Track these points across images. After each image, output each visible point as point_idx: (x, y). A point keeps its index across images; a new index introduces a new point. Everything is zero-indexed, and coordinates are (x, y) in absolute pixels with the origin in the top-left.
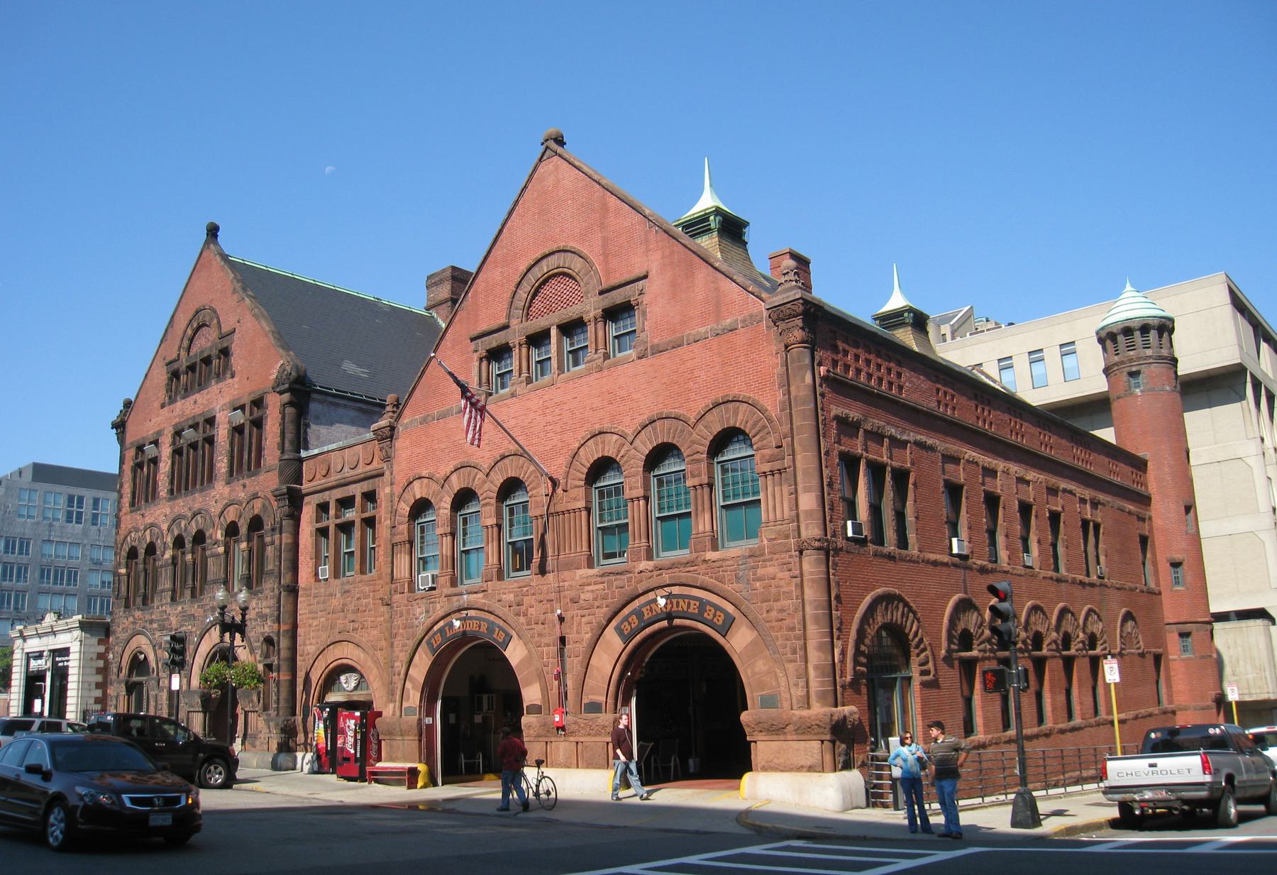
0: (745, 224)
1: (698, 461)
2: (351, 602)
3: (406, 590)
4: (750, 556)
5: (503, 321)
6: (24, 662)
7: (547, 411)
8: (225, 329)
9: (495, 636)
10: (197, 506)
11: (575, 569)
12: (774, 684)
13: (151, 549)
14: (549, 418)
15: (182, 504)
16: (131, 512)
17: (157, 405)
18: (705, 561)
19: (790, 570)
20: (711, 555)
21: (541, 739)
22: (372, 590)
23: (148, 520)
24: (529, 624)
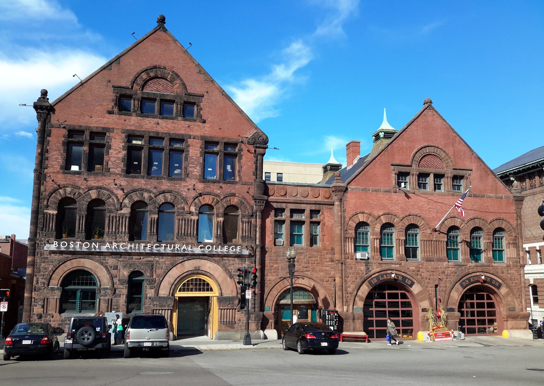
1: (490, 235)
2: (304, 258)
4: (507, 267)
5: (409, 163)
7: (430, 203)
9: (406, 282)
14: (431, 206)
18: (492, 266)
24: (422, 278)
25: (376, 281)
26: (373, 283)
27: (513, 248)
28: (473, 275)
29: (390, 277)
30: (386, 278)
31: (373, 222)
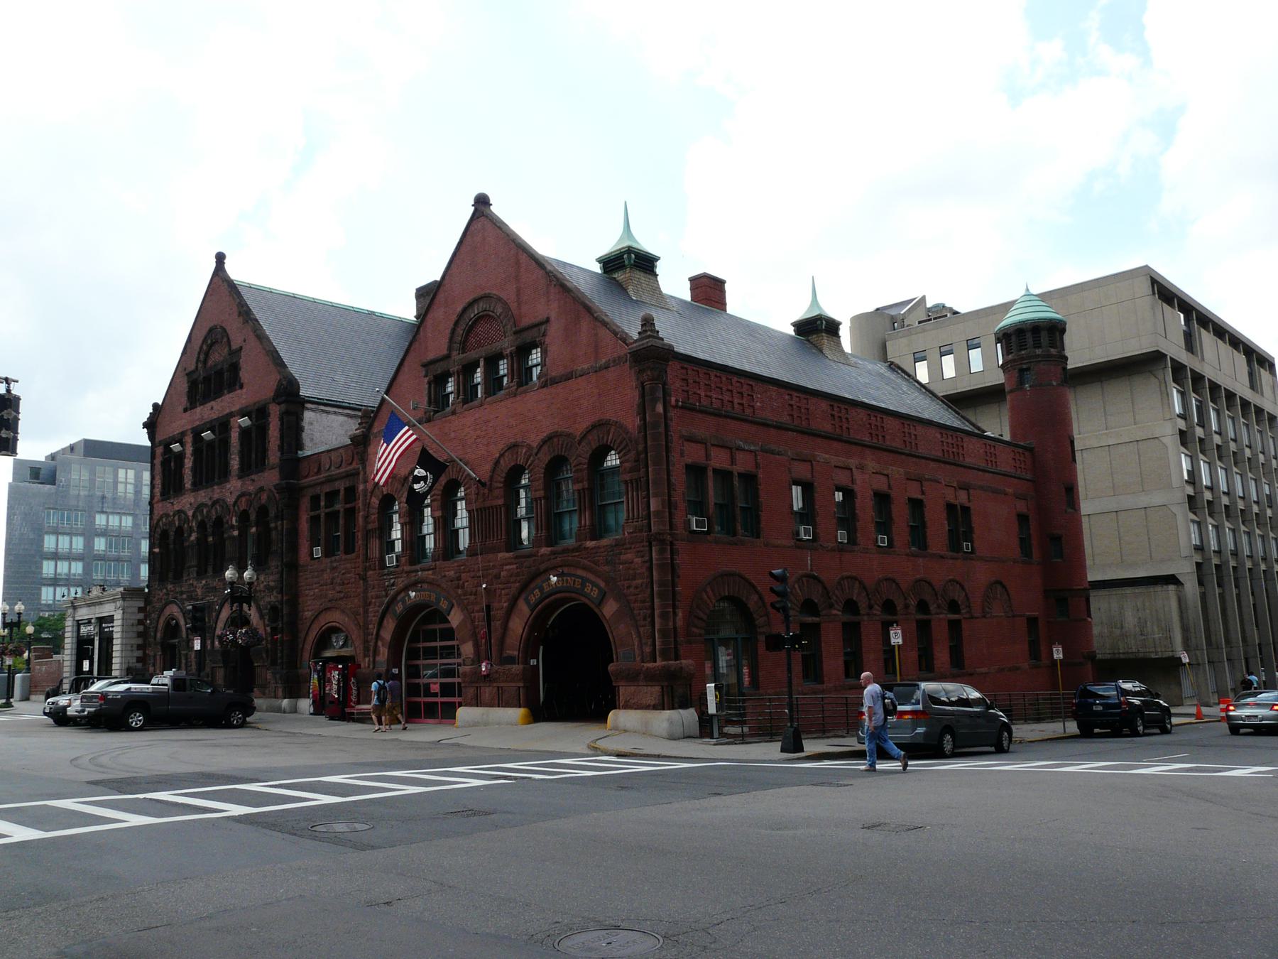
0: (656, 259)
1: (581, 470)
3: (377, 568)
4: (616, 545)
6: (75, 628)
8: (234, 347)
10: (216, 496)
13: (180, 531)
15: (203, 494)
16: (162, 500)
17: (181, 409)
19: (643, 557)
20: (590, 544)
21: (474, 685)
22: (353, 566)
23: (176, 508)
26: (398, 611)
31: (399, 492)
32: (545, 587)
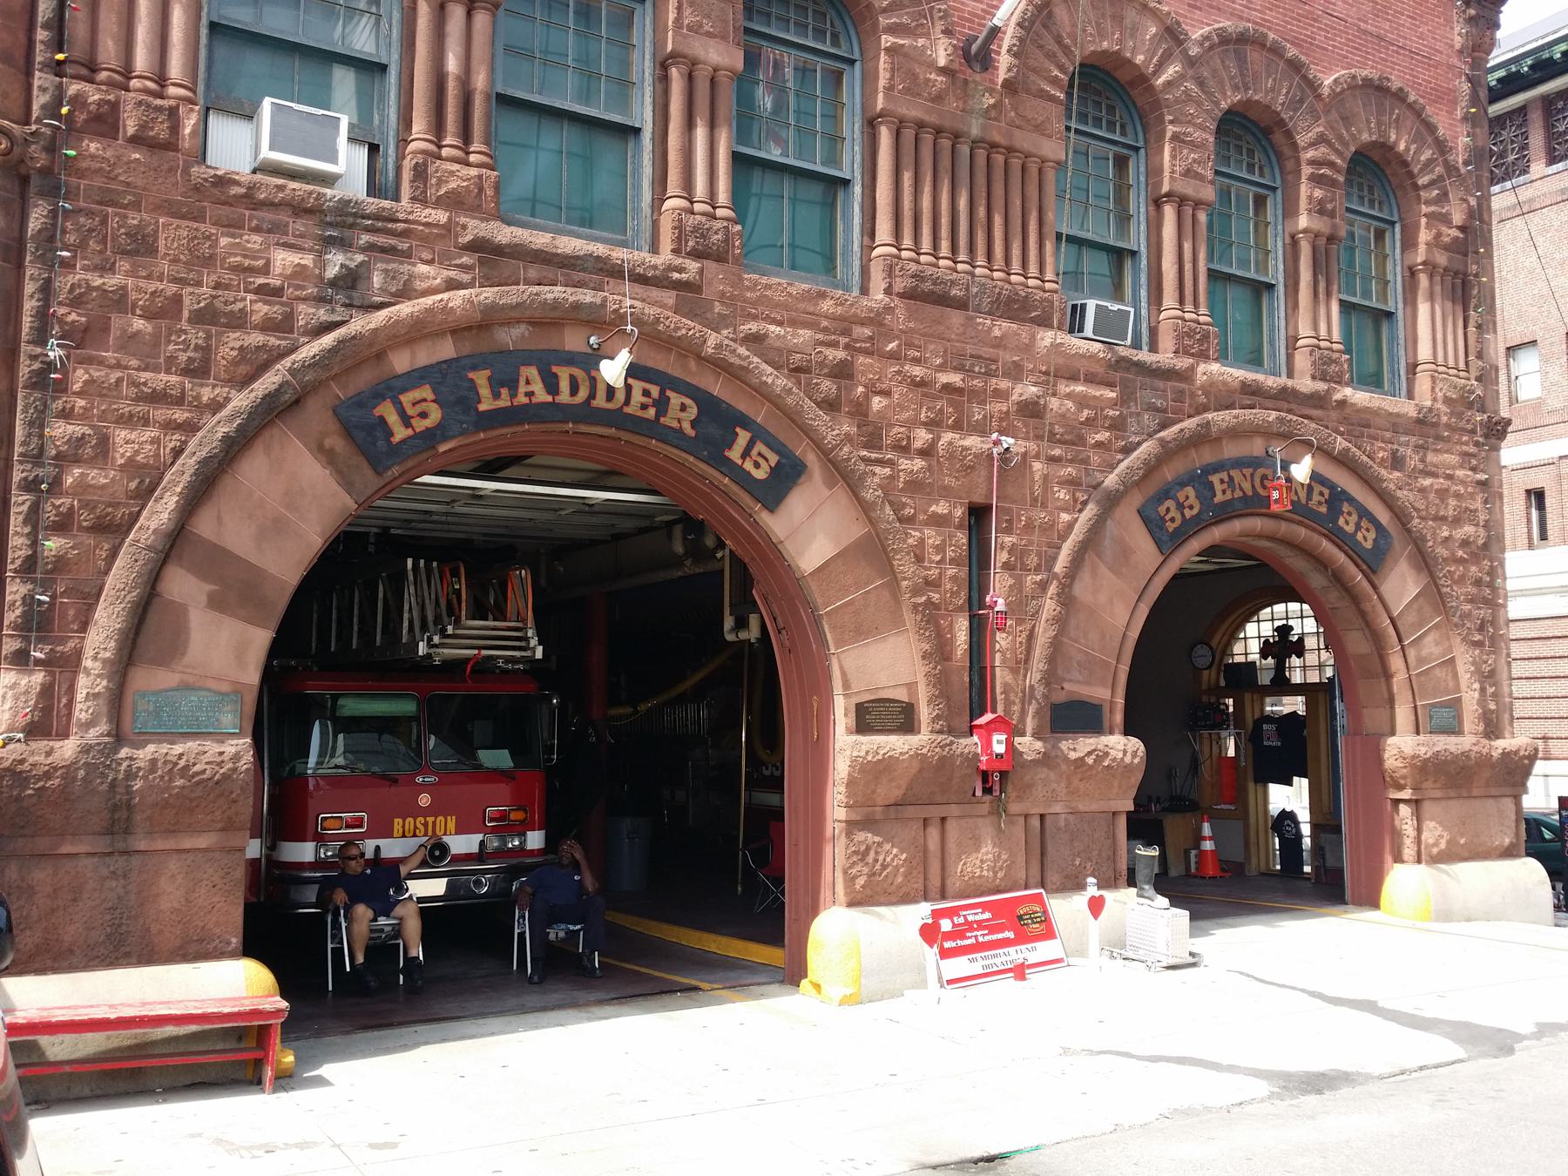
9: (735, 454)
11: (1033, 321)
12: (1451, 684)
20: (1360, 397)
21: (910, 811)
25: (435, 415)
27: (1449, 305)
28: (1231, 450)
29: (583, 394)
30: (542, 396)
32: (1218, 487)
